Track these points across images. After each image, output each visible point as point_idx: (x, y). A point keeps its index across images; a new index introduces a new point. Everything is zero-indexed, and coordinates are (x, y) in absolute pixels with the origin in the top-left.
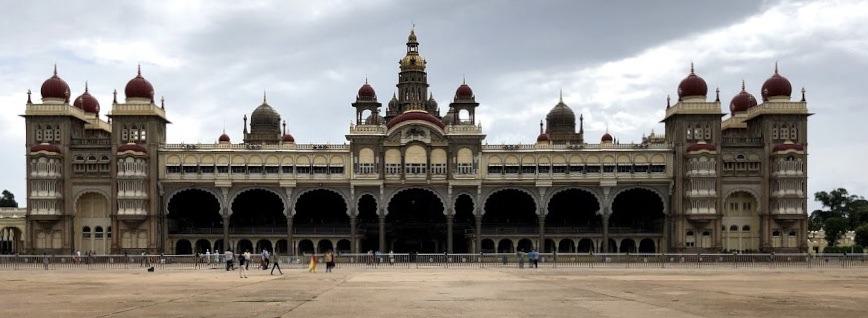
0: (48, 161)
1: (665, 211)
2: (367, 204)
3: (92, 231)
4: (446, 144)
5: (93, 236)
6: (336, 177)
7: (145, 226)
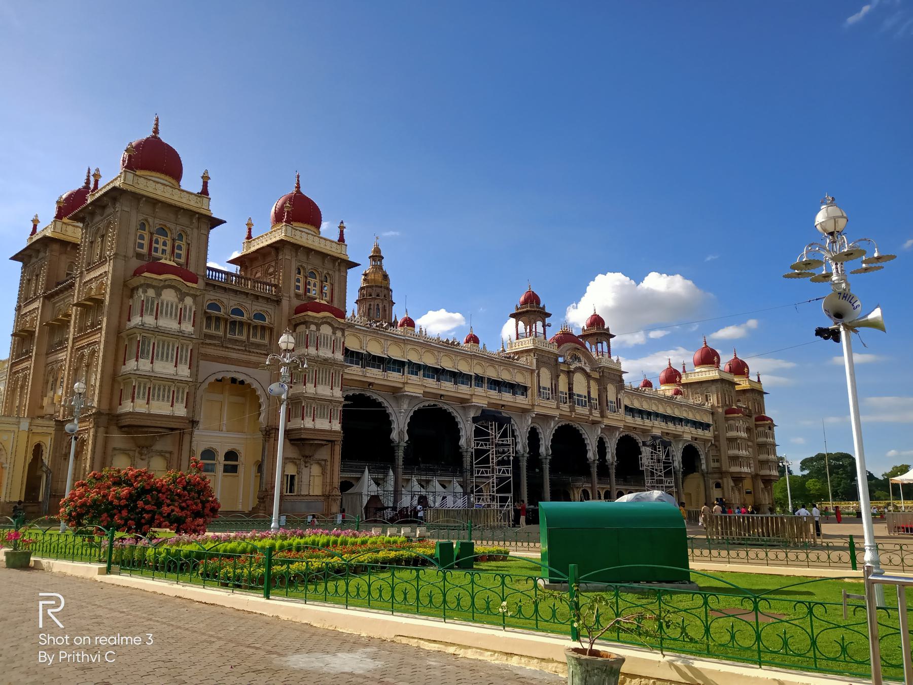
0: (182, 300)
1: (704, 467)
6: (521, 400)
7: (324, 454)
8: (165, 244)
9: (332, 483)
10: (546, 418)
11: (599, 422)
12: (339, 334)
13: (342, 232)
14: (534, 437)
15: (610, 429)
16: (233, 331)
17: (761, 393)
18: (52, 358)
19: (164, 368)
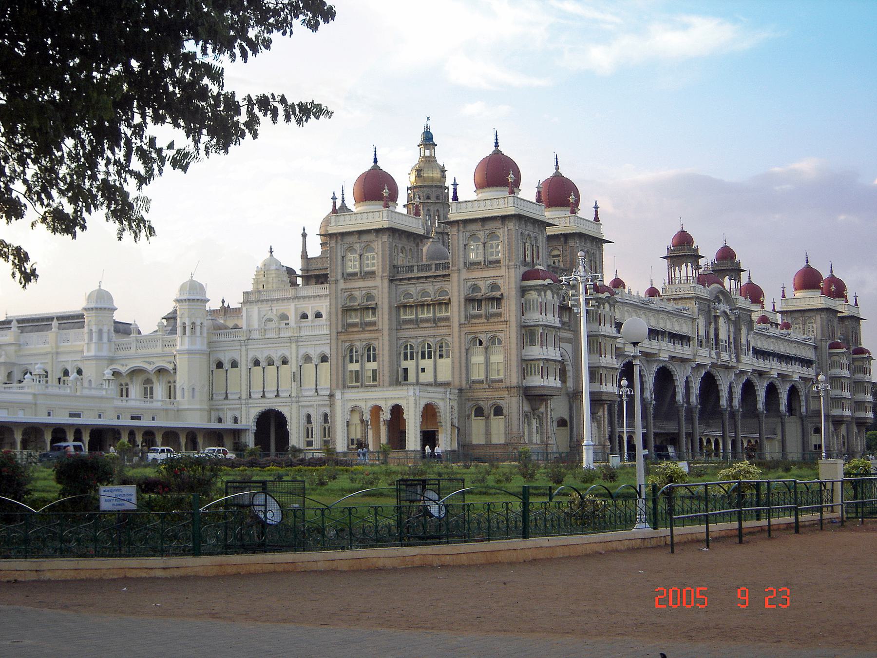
1: (803, 409)
4: (733, 319)
9: (604, 434)
11: (732, 367)
13: (596, 212)
15: (742, 372)
17: (857, 319)
18: (403, 334)
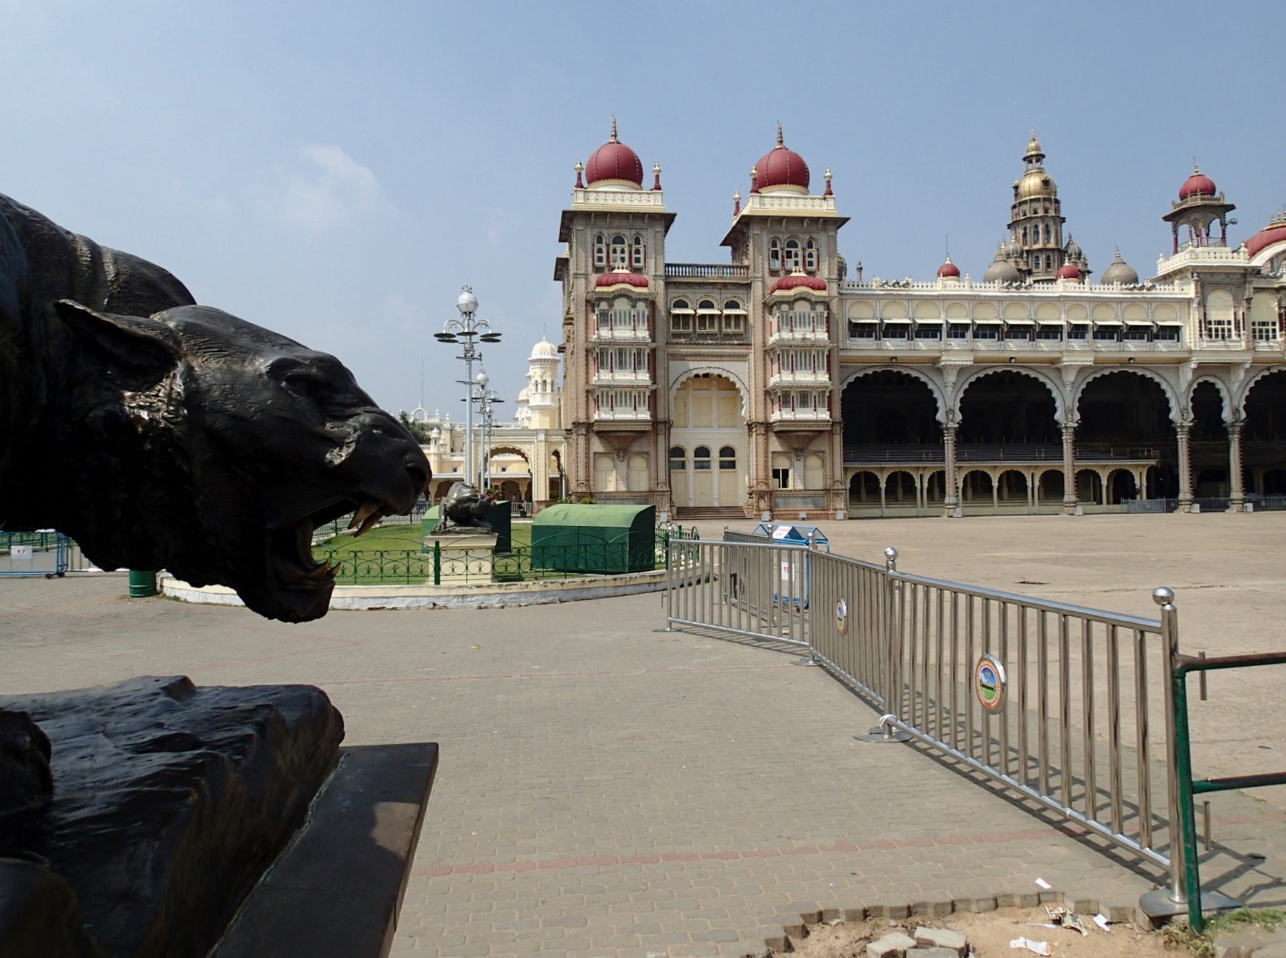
0: (634, 307)
2: (1206, 399)
3: (690, 456)
5: (690, 466)
7: (821, 444)
8: (623, 251)
10: (1227, 368)
12: (820, 308)
14: (1206, 399)
16: (703, 325)
19: (624, 377)
